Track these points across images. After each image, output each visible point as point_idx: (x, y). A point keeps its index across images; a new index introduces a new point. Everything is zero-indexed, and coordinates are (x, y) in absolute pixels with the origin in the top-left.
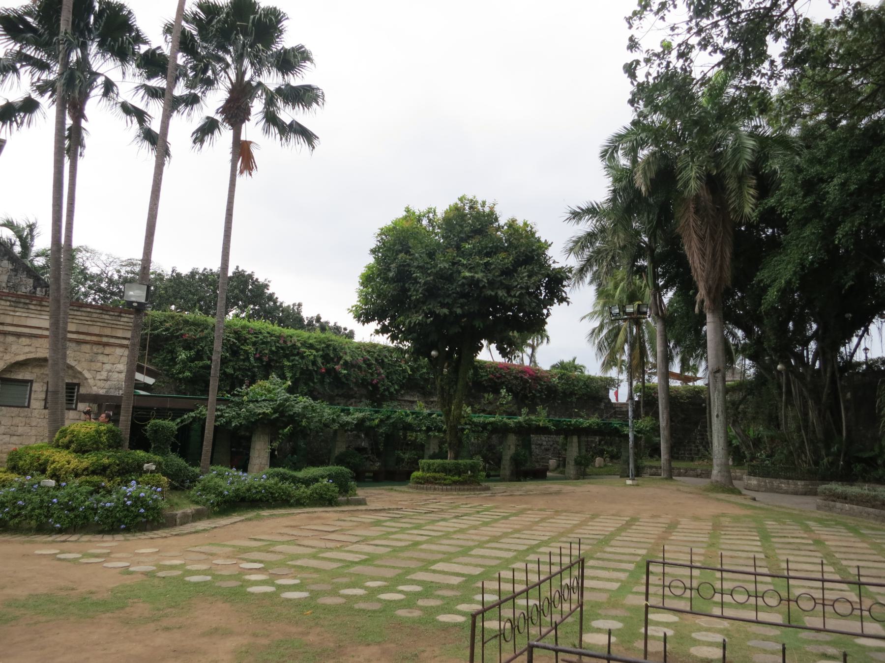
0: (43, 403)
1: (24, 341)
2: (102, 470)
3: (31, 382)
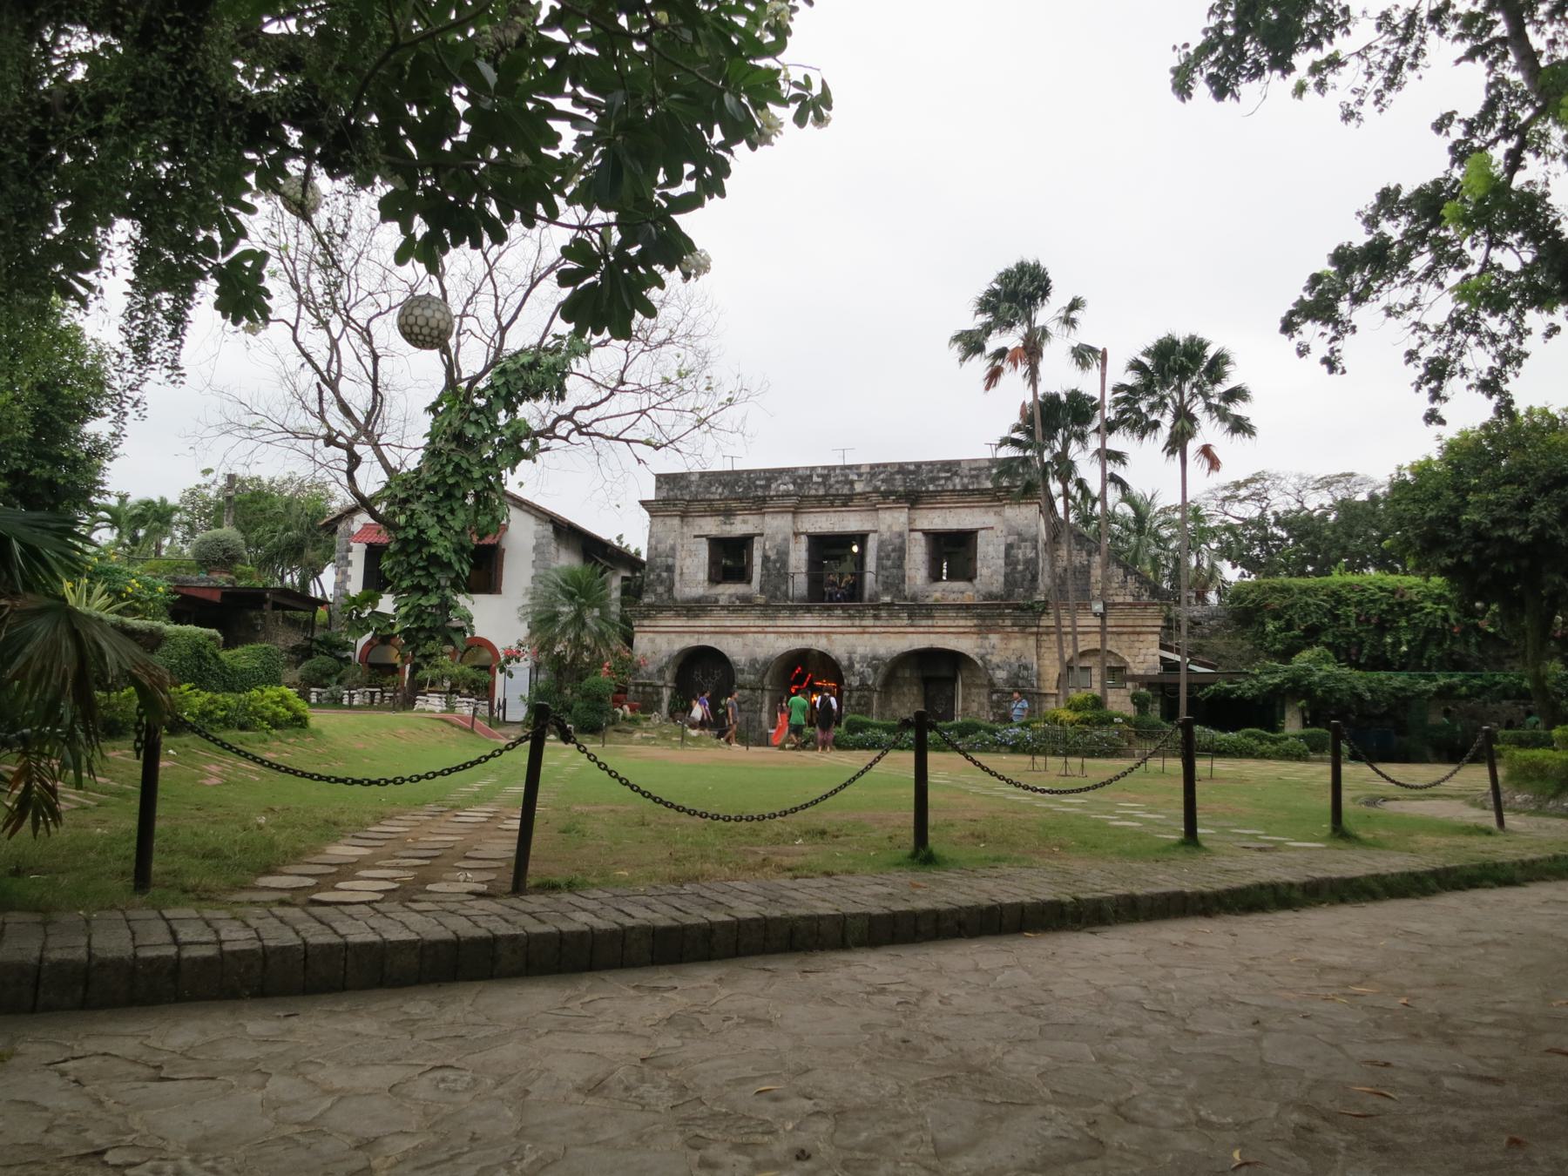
2: (1087, 721)
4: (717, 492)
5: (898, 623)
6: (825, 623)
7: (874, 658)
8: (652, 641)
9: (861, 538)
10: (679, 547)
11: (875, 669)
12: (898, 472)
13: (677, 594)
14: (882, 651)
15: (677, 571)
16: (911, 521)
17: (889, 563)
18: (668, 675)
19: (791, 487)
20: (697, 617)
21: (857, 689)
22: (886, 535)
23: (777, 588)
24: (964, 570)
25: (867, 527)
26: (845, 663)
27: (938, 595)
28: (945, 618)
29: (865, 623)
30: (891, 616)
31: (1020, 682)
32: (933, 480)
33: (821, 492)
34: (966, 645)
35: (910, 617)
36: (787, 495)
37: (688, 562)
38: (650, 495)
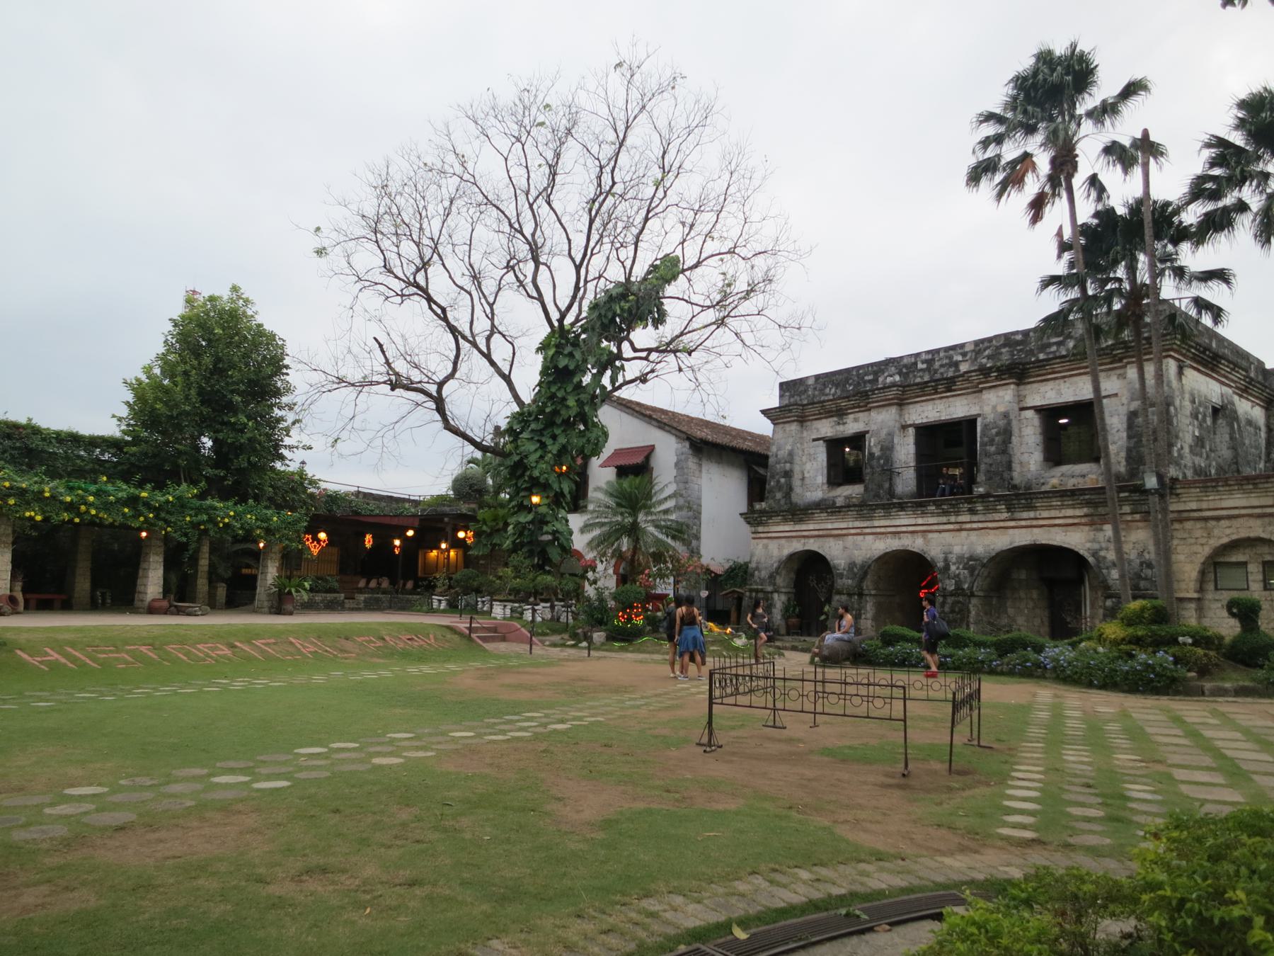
0: (1262, 585)
1: (1224, 523)
2: (1137, 641)
3: (1245, 564)
4: (831, 391)
5: (997, 516)
6: (920, 521)
7: (971, 558)
8: (766, 547)
9: (971, 422)
10: (796, 451)
11: (972, 570)
12: (1004, 345)
14: (979, 550)
16: (1020, 398)
17: (993, 449)
18: (780, 581)
19: (897, 378)
20: (801, 521)
21: (952, 594)
22: (990, 418)
23: (880, 486)
24: (1093, 452)
25: (974, 411)
26: (941, 564)
27: (1055, 481)
28: (1050, 508)
29: (961, 519)
30: (988, 510)
31: (1142, 584)
32: (1043, 348)
33: (926, 378)
34: (1076, 539)
35: (1009, 510)
36: (894, 385)
37: (808, 466)
38: (774, 402)
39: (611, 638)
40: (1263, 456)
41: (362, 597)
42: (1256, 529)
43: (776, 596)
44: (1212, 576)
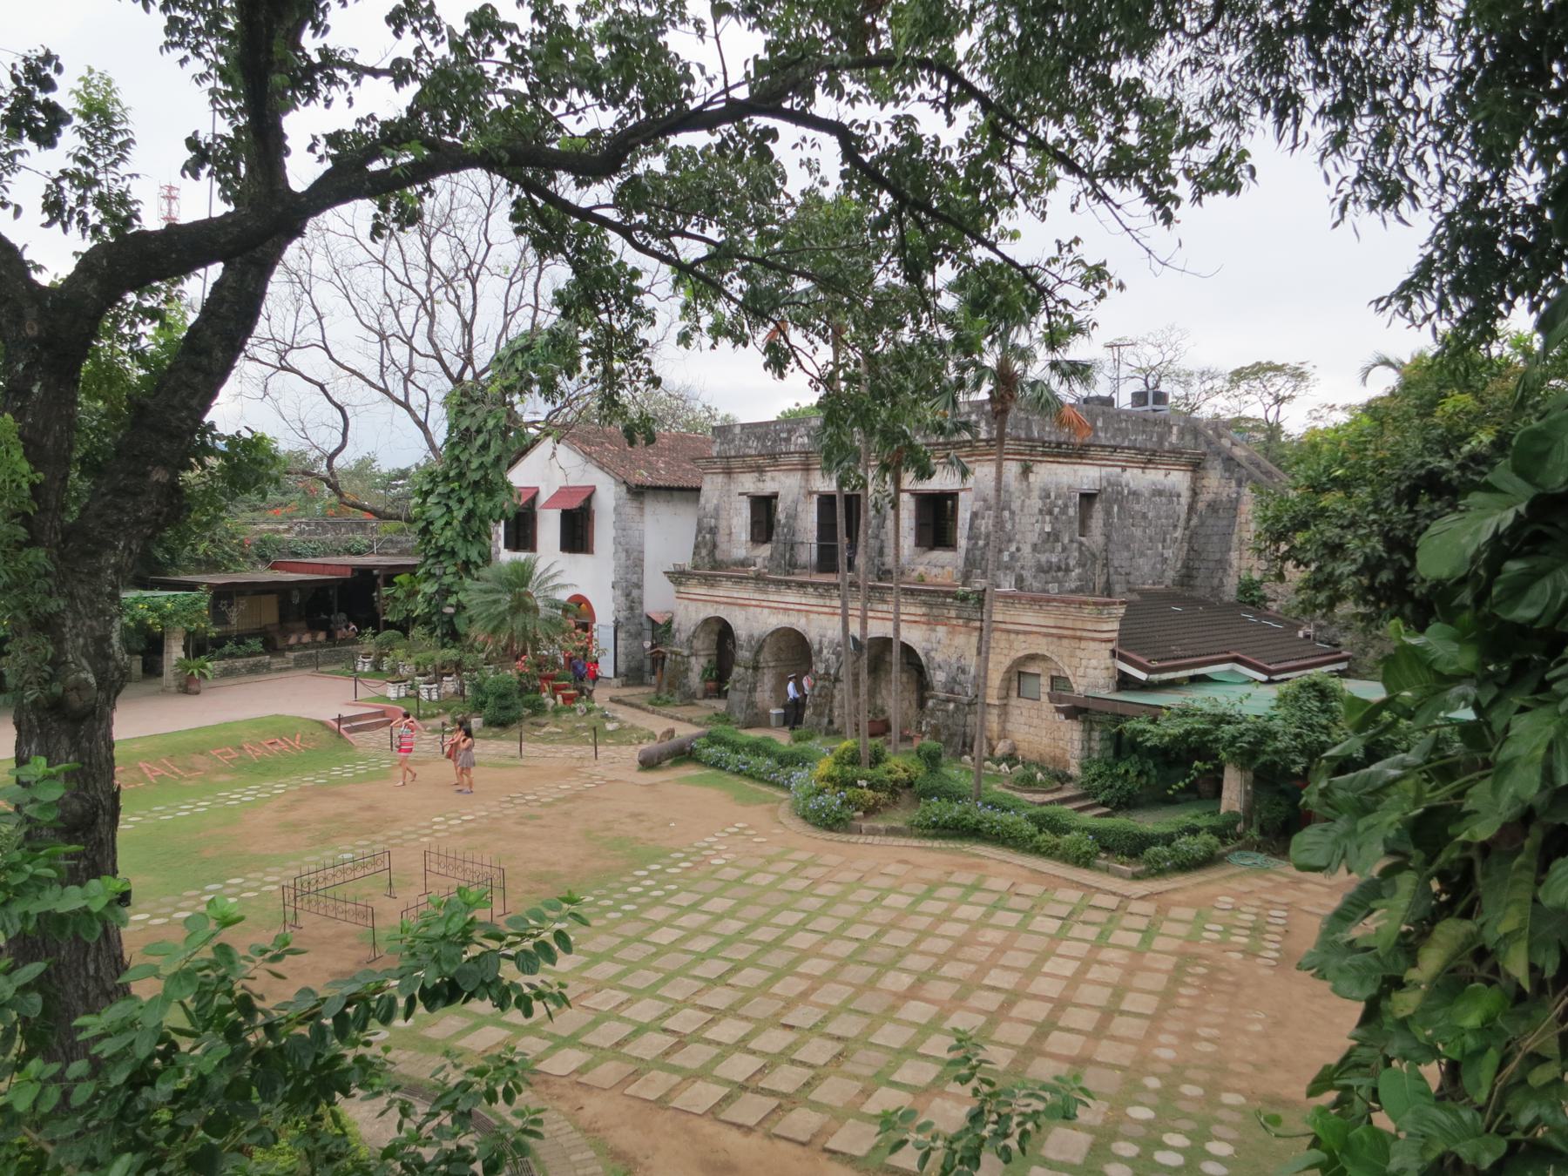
1: (1021, 637)
8: (686, 608)
13: (719, 555)
15: (723, 531)
26: (816, 647)
27: (921, 569)
31: (957, 688)
39: (489, 723)
40: (1182, 523)
41: (291, 655)
42: (1040, 646)
43: (693, 660)
44: (1015, 684)
